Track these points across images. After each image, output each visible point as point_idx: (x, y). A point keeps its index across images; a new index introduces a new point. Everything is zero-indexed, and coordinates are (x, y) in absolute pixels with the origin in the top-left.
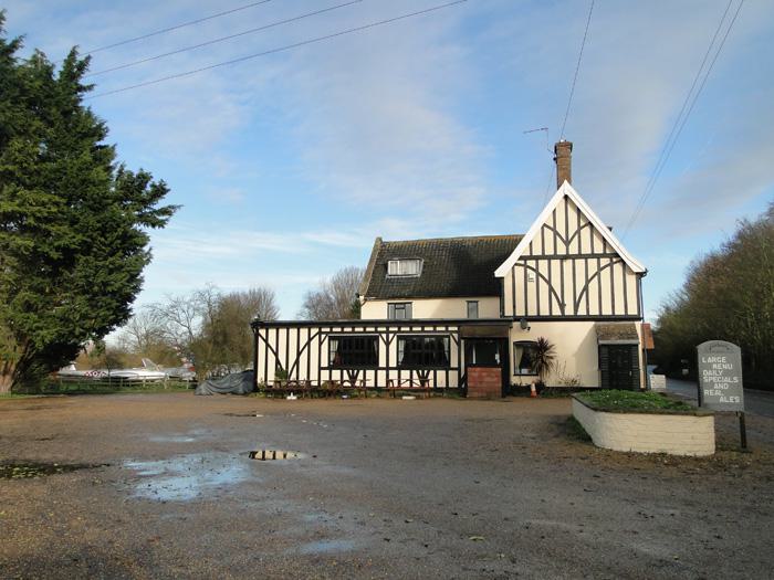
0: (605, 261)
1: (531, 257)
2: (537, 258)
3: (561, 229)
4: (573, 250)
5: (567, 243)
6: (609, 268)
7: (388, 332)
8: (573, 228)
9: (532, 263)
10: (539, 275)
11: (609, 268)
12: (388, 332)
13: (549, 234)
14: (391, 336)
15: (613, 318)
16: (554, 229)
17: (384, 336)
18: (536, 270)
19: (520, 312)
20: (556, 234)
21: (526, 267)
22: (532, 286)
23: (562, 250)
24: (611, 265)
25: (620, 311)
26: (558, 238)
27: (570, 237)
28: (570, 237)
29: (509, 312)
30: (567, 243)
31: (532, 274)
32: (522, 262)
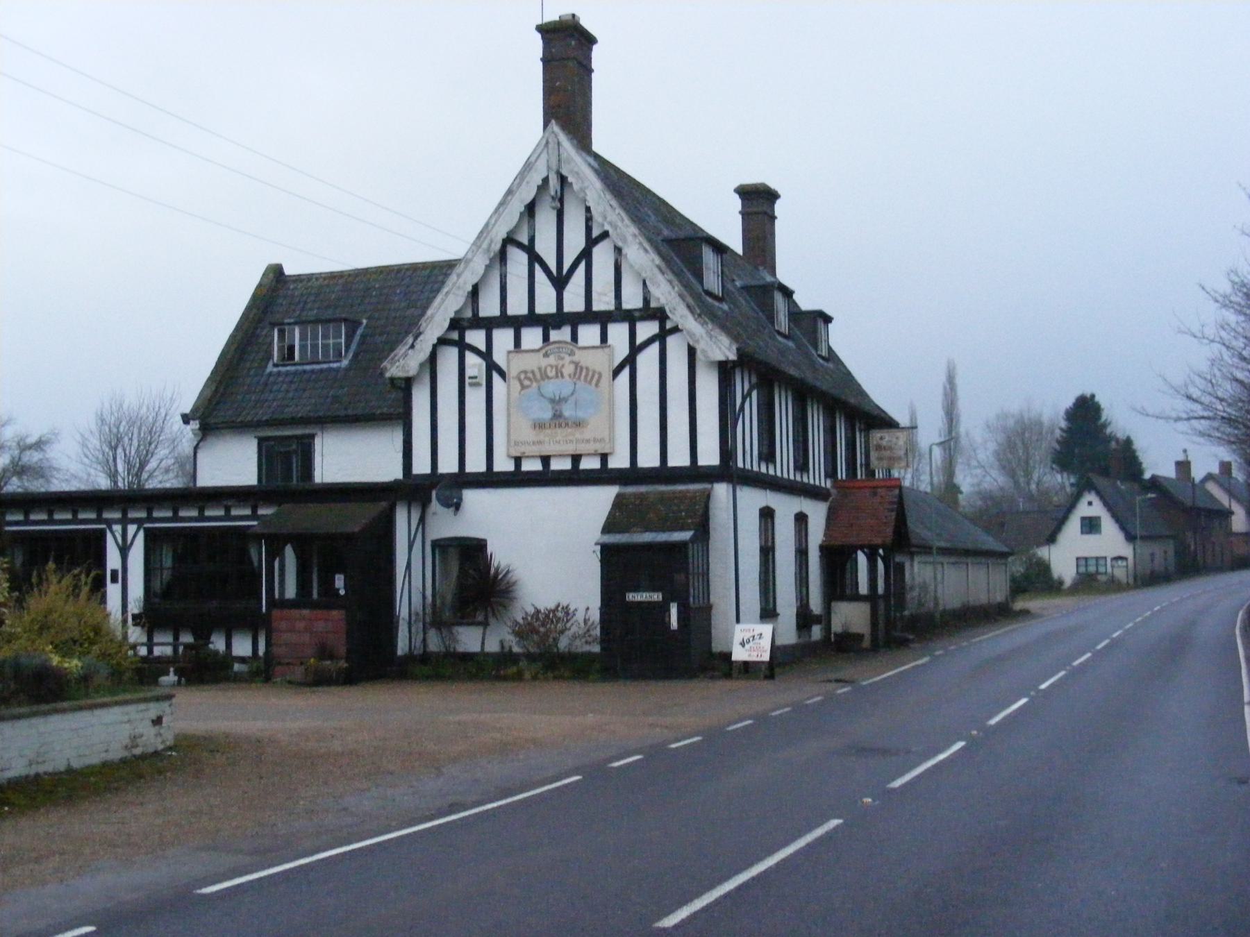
0: (646, 330)
1: (479, 322)
2: (489, 325)
3: (546, 247)
4: (574, 301)
5: (560, 282)
6: (655, 347)
7: (124, 522)
8: (575, 242)
9: (476, 338)
10: (492, 367)
11: (655, 347)
12: (124, 522)
13: (518, 261)
14: (132, 529)
15: (664, 474)
16: (530, 249)
17: (117, 528)
18: (487, 355)
19: (448, 465)
20: (535, 258)
21: (463, 347)
22: (475, 398)
23: (546, 303)
24: (661, 337)
25: (679, 458)
26: (537, 267)
27: (567, 265)
28: (567, 265)
29: (421, 466)
30: (560, 282)
31: (474, 364)
32: (455, 335)
